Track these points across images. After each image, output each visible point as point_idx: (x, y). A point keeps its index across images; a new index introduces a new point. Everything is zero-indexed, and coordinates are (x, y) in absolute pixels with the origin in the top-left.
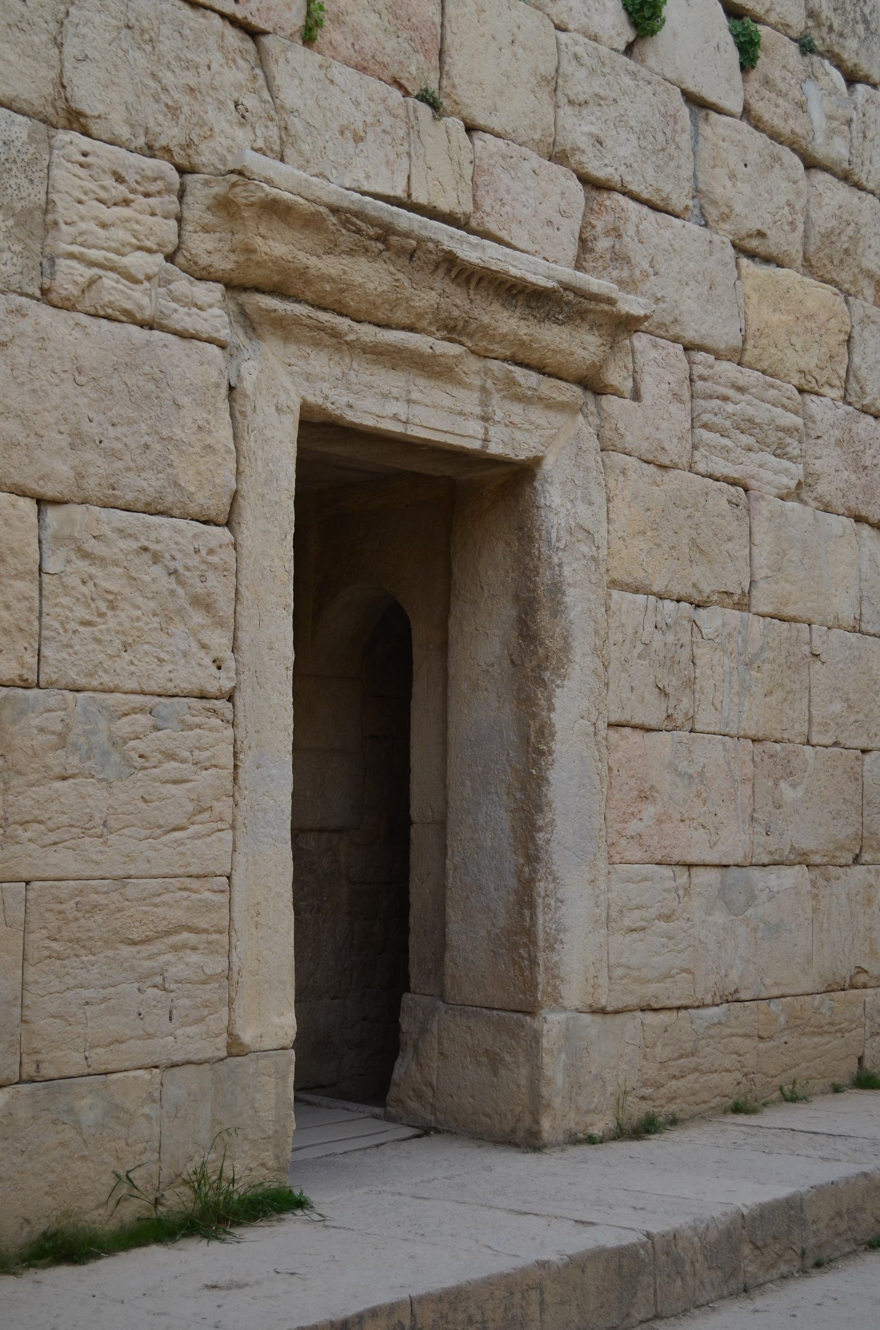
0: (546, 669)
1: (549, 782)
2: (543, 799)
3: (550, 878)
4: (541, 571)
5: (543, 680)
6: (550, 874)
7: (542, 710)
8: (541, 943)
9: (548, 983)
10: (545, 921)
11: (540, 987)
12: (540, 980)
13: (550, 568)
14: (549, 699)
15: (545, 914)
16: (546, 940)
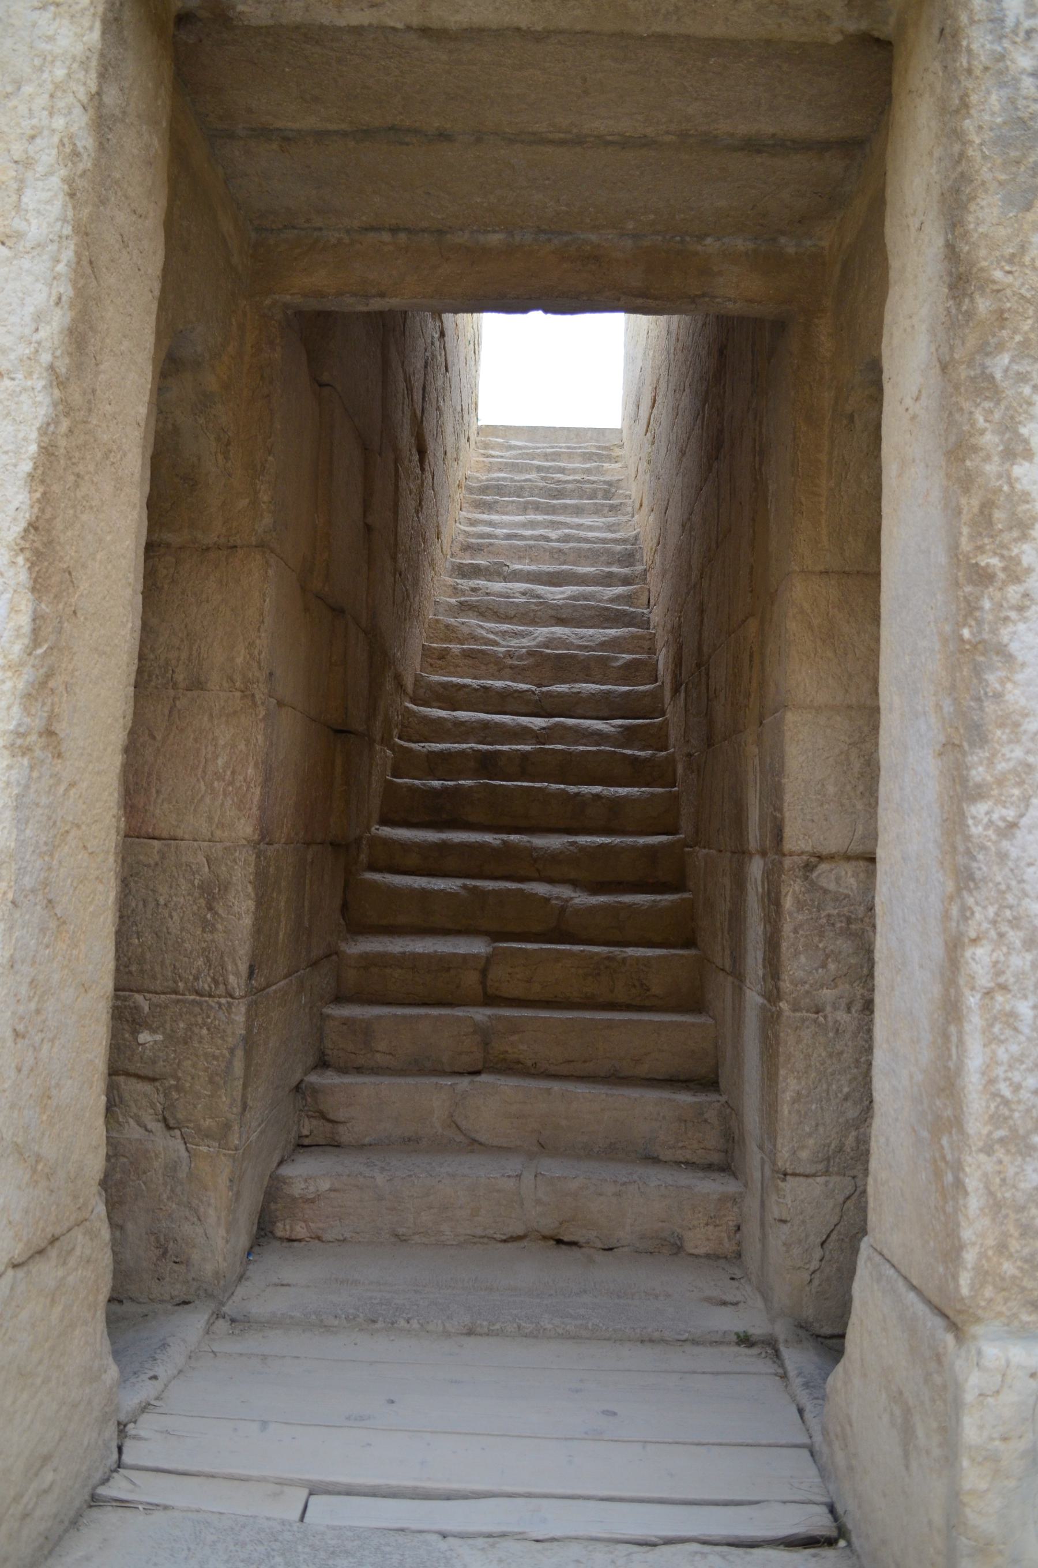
0: (1000, 347)
1: (1008, 658)
2: (989, 707)
3: (1015, 937)
4: (974, 98)
5: (991, 378)
6: (1015, 923)
7: (988, 458)
8: (976, 1126)
9: (1002, 1248)
10: (993, 1061)
11: (970, 1256)
12: (967, 1234)
13: (1002, 85)
14: (1009, 427)
15: (991, 1041)
16: (996, 1120)
